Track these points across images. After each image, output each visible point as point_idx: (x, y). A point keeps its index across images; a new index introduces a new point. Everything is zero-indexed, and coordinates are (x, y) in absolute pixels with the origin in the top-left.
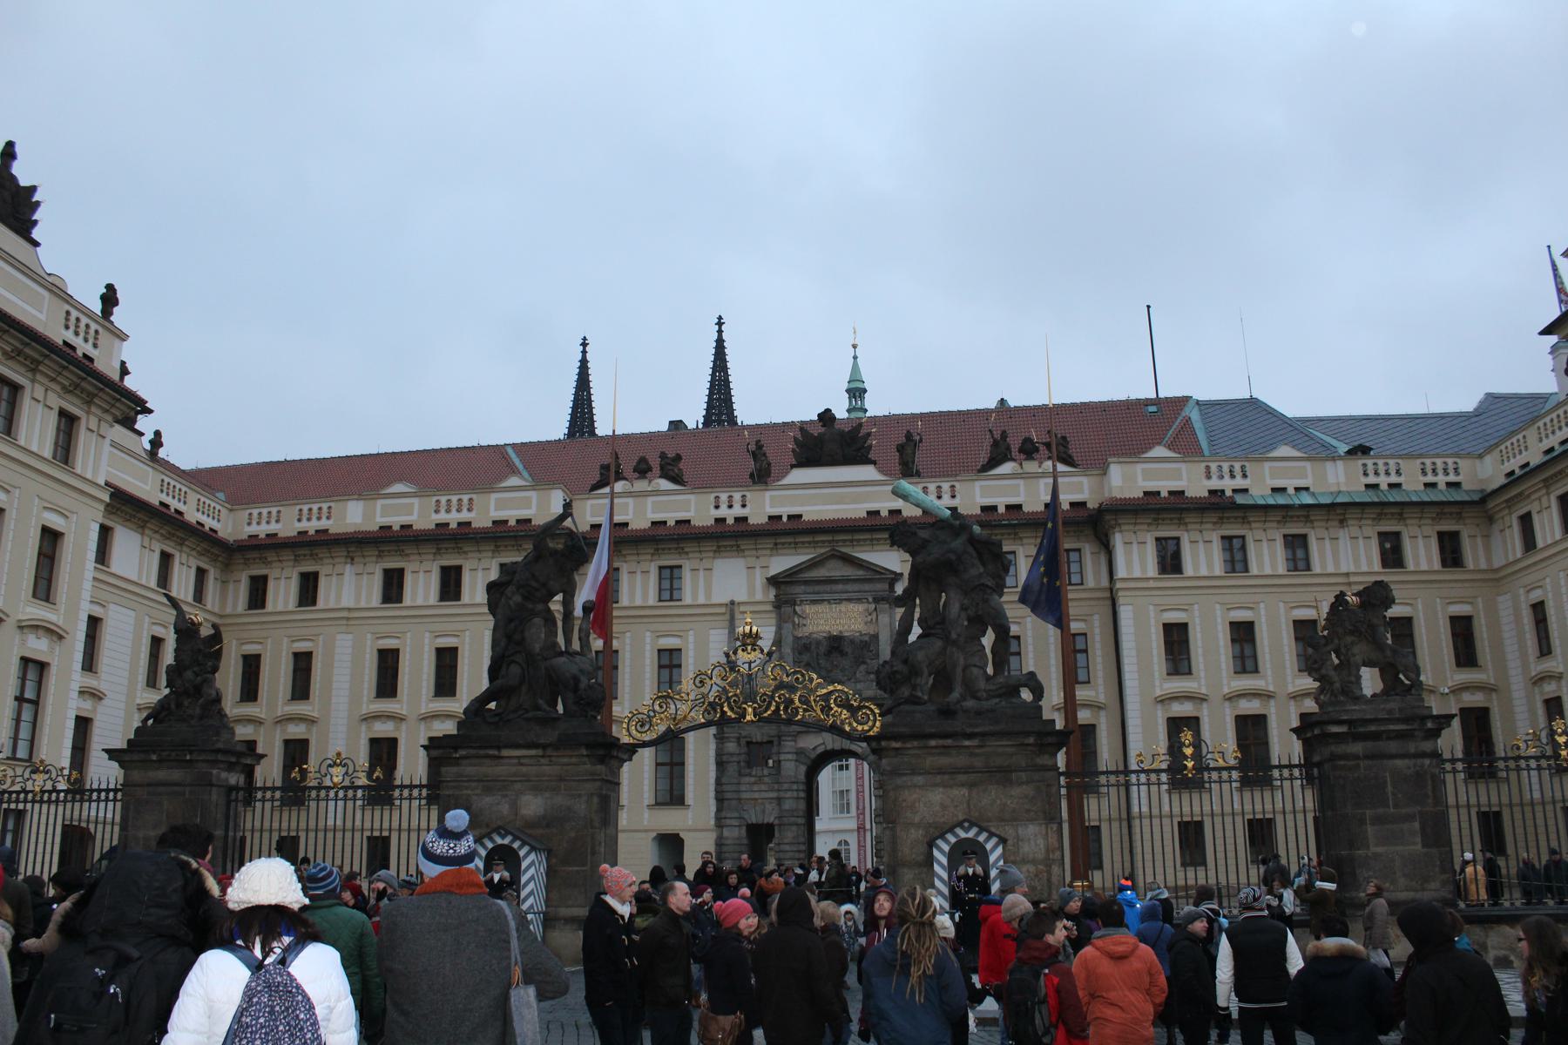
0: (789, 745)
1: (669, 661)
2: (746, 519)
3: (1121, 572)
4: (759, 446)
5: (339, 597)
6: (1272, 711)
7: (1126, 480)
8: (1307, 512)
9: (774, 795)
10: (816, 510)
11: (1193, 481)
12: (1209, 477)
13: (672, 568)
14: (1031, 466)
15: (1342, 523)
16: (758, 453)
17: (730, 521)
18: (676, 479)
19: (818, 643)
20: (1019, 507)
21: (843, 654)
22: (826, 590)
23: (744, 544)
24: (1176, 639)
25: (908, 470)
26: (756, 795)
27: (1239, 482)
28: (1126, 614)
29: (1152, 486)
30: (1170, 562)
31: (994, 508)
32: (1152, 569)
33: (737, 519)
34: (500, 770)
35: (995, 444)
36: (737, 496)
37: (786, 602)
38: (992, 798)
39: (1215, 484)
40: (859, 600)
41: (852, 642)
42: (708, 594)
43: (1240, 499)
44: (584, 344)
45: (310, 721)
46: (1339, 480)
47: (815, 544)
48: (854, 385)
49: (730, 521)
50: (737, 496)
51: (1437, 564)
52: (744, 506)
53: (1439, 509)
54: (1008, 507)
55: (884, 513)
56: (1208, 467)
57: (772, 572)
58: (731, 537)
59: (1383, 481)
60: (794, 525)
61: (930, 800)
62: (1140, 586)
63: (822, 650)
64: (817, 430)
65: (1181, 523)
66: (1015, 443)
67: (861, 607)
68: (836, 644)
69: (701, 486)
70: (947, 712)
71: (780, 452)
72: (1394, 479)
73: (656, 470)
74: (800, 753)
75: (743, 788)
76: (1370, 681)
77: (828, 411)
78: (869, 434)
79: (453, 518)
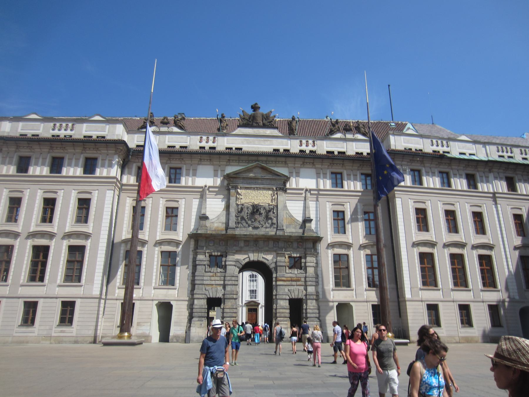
0: (230, 258)
1: (171, 213)
2: (214, 148)
4: (223, 117)
9: (222, 282)
12: (432, 145)
13: (176, 169)
14: (349, 136)
15: (490, 171)
17: (207, 148)
18: (181, 128)
19: (248, 208)
20: (344, 153)
21: (260, 214)
22: (253, 183)
24: (421, 216)
26: (213, 282)
27: (445, 149)
31: (333, 152)
33: (210, 148)
37: (233, 187)
39: (435, 148)
40: (269, 189)
41: (264, 208)
42: (193, 182)
47: (249, 162)
49: (207, 148)
52: (213, 142)
54: (339, 153)
55: (281, 151)
56: (432, 141)
63: (250, 211)
67: (270, 192)
68: (256, 209)
72: (509, 154)
73: (173, 122)
74: (237, 261)
75: (205, 278)
77: (256, 104)
78: (275, 116)
79: (62, 133)
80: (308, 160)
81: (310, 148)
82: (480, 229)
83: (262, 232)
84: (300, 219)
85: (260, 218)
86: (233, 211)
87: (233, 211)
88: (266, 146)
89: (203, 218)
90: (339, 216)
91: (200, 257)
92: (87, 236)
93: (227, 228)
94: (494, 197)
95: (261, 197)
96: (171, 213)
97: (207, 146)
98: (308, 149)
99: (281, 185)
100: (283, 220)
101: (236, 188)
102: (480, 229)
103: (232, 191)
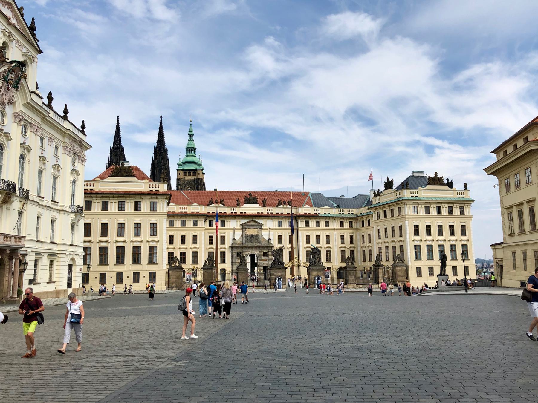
0: (244, 253)
7: (302, 211)
8: (329, 218)
11: (311, 211)
14: (285, 206)
16: (238, 200)
18: (223, 205)
22: (251, 226)
24: (308, 237)
25: (264, 205)
27: (319, 212)
28: (300, 233)
29: (305, 212)
30: (307, 224)
32: (305, 226)
38: (319, 273)
39: (315, 212)
43: (319, 215)
44: (118, 118)
46: (335, 212)
48: (190, 133)
57: (242, 223)
58: (234, 216)
59: (341, 213)
60: (245, 215)
61: (314, 274)
64: (248, 197)
66: (282, 201)
68: (252, 236)
69: (228, 206)
71: (242, 200)
76: (350, 264)
79: (183, 211)
80: (270, 216)
81: (271, 212)
82: (328, 242)
83: (254, 244)
88: (255, 212)
89: (234, 240)
90: (280, 238)
91: (234, 253)
92: (198, 248)
95: (253, 231)
96: (223, 238)
97: (234, 212)
98: (270, 212)
99: (260, 226)
101: (245, 229)
102: (328, 242)
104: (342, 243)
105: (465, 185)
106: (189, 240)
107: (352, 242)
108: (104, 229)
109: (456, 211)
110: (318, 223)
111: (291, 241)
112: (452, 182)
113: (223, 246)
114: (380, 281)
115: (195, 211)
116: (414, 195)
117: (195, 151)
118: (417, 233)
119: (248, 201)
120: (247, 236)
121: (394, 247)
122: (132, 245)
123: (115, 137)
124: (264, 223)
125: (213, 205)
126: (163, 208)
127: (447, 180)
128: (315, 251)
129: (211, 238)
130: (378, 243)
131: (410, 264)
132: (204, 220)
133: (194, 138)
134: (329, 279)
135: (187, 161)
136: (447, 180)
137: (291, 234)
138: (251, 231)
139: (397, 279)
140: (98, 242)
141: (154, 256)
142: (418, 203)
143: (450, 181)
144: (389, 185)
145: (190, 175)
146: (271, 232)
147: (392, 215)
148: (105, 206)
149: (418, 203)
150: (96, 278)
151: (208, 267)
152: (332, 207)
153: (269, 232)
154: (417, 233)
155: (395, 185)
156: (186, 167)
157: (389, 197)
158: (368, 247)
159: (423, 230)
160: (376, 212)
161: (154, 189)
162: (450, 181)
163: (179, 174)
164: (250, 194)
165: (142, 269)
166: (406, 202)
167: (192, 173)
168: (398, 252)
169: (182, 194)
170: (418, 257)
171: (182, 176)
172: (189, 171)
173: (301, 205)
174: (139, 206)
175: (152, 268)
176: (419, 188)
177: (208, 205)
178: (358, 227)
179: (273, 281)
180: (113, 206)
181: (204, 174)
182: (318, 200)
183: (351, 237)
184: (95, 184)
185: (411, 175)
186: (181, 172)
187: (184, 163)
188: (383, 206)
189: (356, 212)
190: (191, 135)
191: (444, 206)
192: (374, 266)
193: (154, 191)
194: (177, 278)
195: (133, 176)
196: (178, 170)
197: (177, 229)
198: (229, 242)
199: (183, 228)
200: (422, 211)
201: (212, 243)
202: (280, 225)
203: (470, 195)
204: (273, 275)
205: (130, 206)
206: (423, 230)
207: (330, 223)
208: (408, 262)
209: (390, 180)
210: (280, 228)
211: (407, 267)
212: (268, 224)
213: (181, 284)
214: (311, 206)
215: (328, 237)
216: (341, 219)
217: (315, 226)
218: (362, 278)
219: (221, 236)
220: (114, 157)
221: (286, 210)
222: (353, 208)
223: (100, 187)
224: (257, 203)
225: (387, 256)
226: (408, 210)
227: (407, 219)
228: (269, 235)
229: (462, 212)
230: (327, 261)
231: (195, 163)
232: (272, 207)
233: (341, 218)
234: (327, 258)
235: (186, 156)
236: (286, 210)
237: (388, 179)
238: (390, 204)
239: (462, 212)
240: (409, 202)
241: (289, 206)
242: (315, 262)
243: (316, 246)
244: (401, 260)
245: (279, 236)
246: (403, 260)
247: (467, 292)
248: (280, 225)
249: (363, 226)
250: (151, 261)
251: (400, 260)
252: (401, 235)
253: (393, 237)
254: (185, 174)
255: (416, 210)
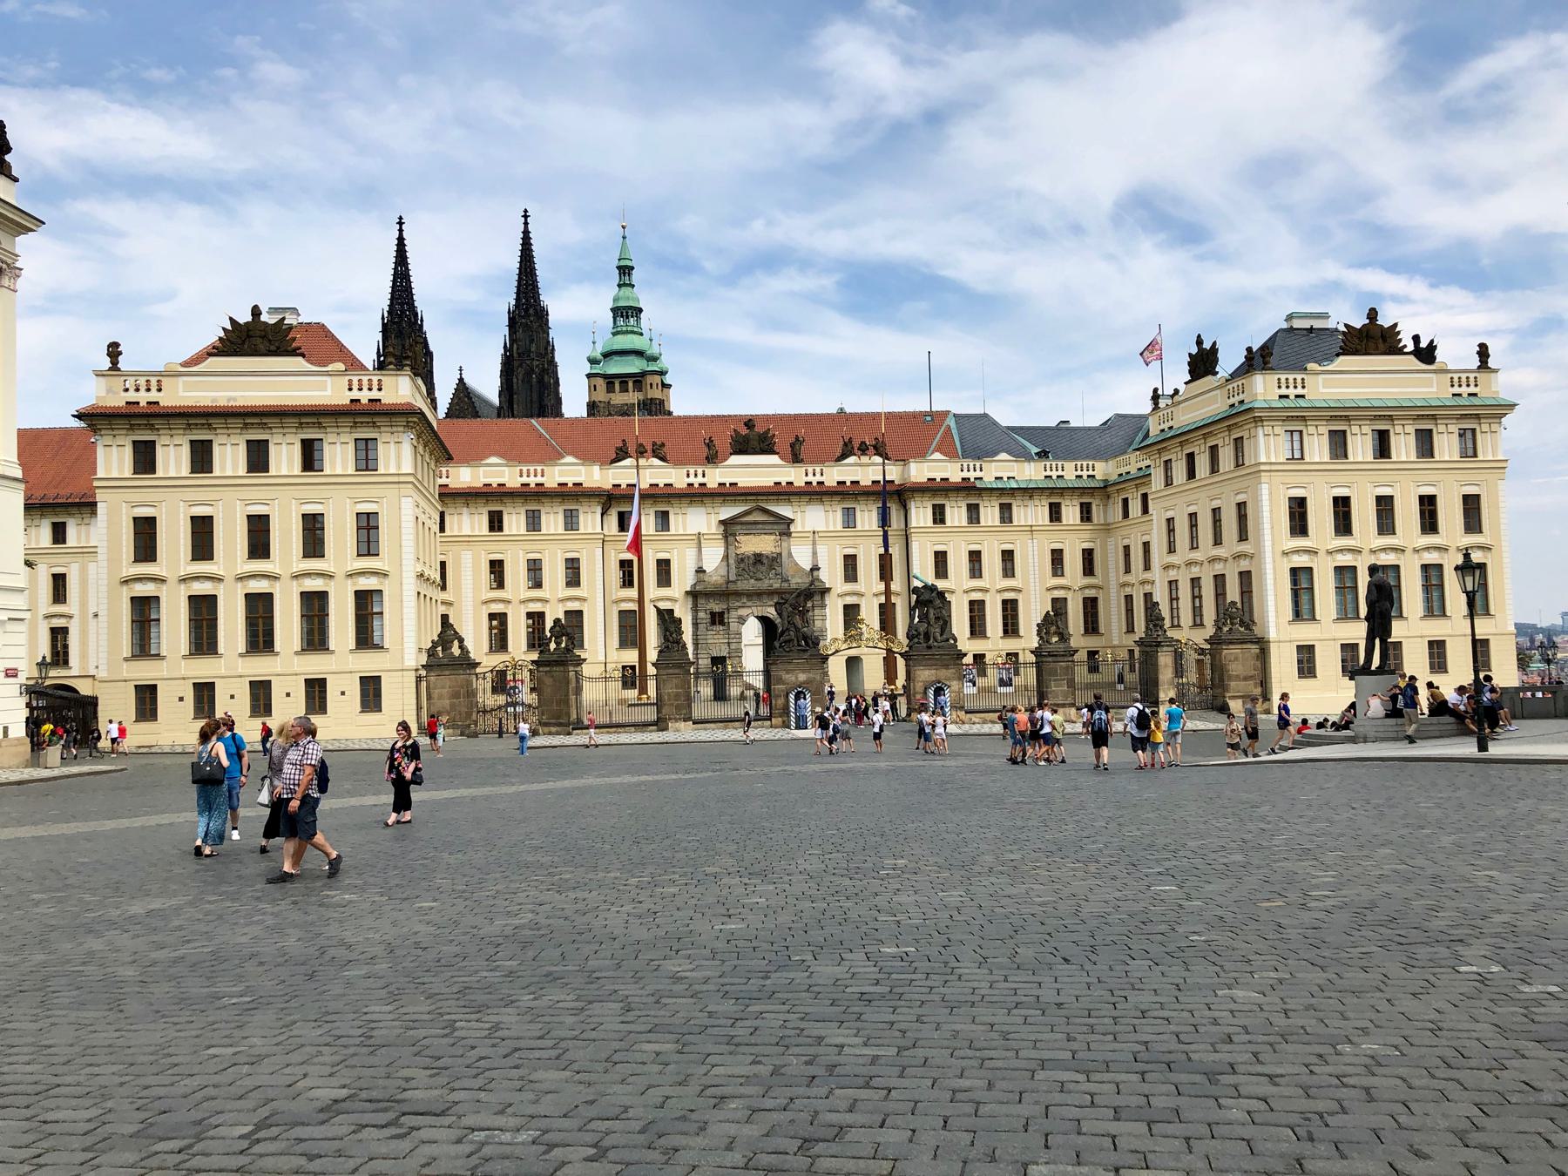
0: (733, 614)
3: (914, 523)
5: (460, 529)
6: (987, 598)
7: (919, 472)
8: (1013, 492)
10: (747, 480)
11: (953, 471)
14: (865, 459)
16: (710, 444)
18: (663, 459)
23: (706, 500)
25: (796, 458)
30: (939, 516)
32: (930, 522)
34: (790, 667)
35: (845, 444)
36: (700, 471)
38: (943, 674)
39: (965, 474)
43: (978, 484)
45: (449, 604)
46: (1031, 473)
48: (623, 263)
50: (700, 471)
51: (1078, 521)
53: (1083, 491)
59: (1054, 474)
61: (925, 674)
62: (924, 531)
64: (744, 431)
65: (947, 496)
68: (758, 558)
69: (679, 462)
70: (929, 647)
71: (723, 442)
79: (532, 481)
80: (816, 494)
81: (818, 478)
82: (1008, 571)
84: (808, 568)
85: (763, 569)
86: (732, 561)
87: (732, 561)
88: (765, 480)
89: (700, 571)
90: (850, 562)
91: (701, 615)
93: (728, 582)
94: (1031, 530)
95: (762, 544)
96: (664, 567)
97: (696, 481)
98: (815, 480)
99: (784, 527)
100: (787, 569)
102: (1008, 571)
103: (731, 539)
104: (1055, 574)
105: (1483, 352)
106: (554, 574)
107: (1088, 569)
108: (202, 535)
109: (1447, 444)
110: (973, 511)
111: (885, 573)
112: (1432, 347)
113: (664, 592)
114: (1162, 696)
115: (570, 480)
116: (1292, 392)
117: (638, 319)
118: (1299, 524)
119: (743, 446)
120: (741, 560)
121: (1220, 580)
122: (296, 588)
123: (394, 281)
124: (798, 517)
125: (628, 462)
126: (399, 457)
127: (1416, 339)
128: (926, 596)
129: (625, 565)
130: (1167, 568)
131: (1272, 635)
132: (599, 510)
133: (636, 276)
134: (1010, 689)
135: (616, 347)
136: (1416, 339)
137: (882, 551)
138: (752, 544)
139: (1225, 688)
140: (183, 580)
141: (376, 623)
142: (1303, 419)
143: (1423, 344)
144: (1203, 363)
145: (624, 389)
146: (817, 541)
147: (1214, 468)
148: (202, 459)
149: (1303, 419)
150: (181, 699)
151: (555, 658)
152: (1022, 455)
153: (814, 543)
154: (1299, 524)
155: (1229, 361)
156: (615, 367)
157: (1210, 403)
158: (1143, 583)
159: (1321, 516)
160: (1160, 462)
161: (364, 396)
162: (1423, 344)
163: (593, 388)
164: (749, 422)
165: (334, 668)
166: (1261, 419)
167: (631, 384)
168: (1233, 593)
169: (535, 429)
170: (1302, 608)
171: (601, 395)
172: (623, 379)
173: (922, 454)
174: (316, 455)
175: (369, 663)
176: (1312, 366)
177: (613, 462)
178: (1110, 520)
179: (781, 701)
180: (230, 455)
181: (666, 386)
182: (978, 436)
183: (1088, 555)
184: (165, 382)
185: (1285, 326)
186: (600, 382)
187: (607, 355)
188: (1182, 437)
189: (1103, 470)
190: (625, 271)
191: (1399, 429)
192: (1140, 643)
193: (364, 401)
194: (456, 695)
195: (294, 352)
196: (589, 376)
197: (514, 540)
198: (683, 579)
199: (534, 536)
200: (1317, 447)
201: (631, 584)
202: (849, 520)
203: (1501, 386)
204: (780, 681)
205: (285, 455)
206: (1321, 516)
207: (1014, 508)
208: (1265, 627)
209: (1207, 345)
210: (849, 532)
211: (1263, 645)
212: (811, 519)
213: (469, 715)
214: (951, 454)
215: (1008, 556)
216: (1053, 496)
217: (964, 523)
218: (1120, 687)
219: (659, 562)
220: (393, 340)
221: (865, 471)
222: (1094, 459)
223: (179, 395)
224: (774, 453)
225: (1197, 612)
226: (1269, 446)
227: (1264, 477)
228: (815, 553)
229: (1469, 449)
230: (1006, 632)
231: (639, 353)
232: (822, 461)
233: (1052, 491)
234: (1005, 625)
235: (614, 334)
236: (865, 471)
237: (1199, 342)
238: (1204, 429)
239: (1469, 449)
240: (1270, 419)
241: (878, 459)
242: (927, 636)
243: (930, 579)
244: (1242, 623)
245: (846, 557)
246: (1248, 624)
247: (1483, 747)
248: (849, 520)
249: (1126, 515)
250: (365, 639)
251: (1238, 621)
252: (1243, 536)
253: (1217, 541)
254: (610, 388)
255: (1297, 445)
